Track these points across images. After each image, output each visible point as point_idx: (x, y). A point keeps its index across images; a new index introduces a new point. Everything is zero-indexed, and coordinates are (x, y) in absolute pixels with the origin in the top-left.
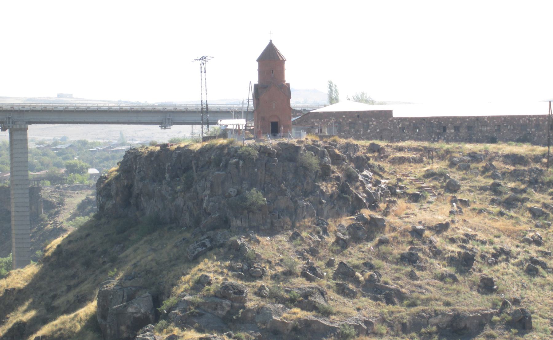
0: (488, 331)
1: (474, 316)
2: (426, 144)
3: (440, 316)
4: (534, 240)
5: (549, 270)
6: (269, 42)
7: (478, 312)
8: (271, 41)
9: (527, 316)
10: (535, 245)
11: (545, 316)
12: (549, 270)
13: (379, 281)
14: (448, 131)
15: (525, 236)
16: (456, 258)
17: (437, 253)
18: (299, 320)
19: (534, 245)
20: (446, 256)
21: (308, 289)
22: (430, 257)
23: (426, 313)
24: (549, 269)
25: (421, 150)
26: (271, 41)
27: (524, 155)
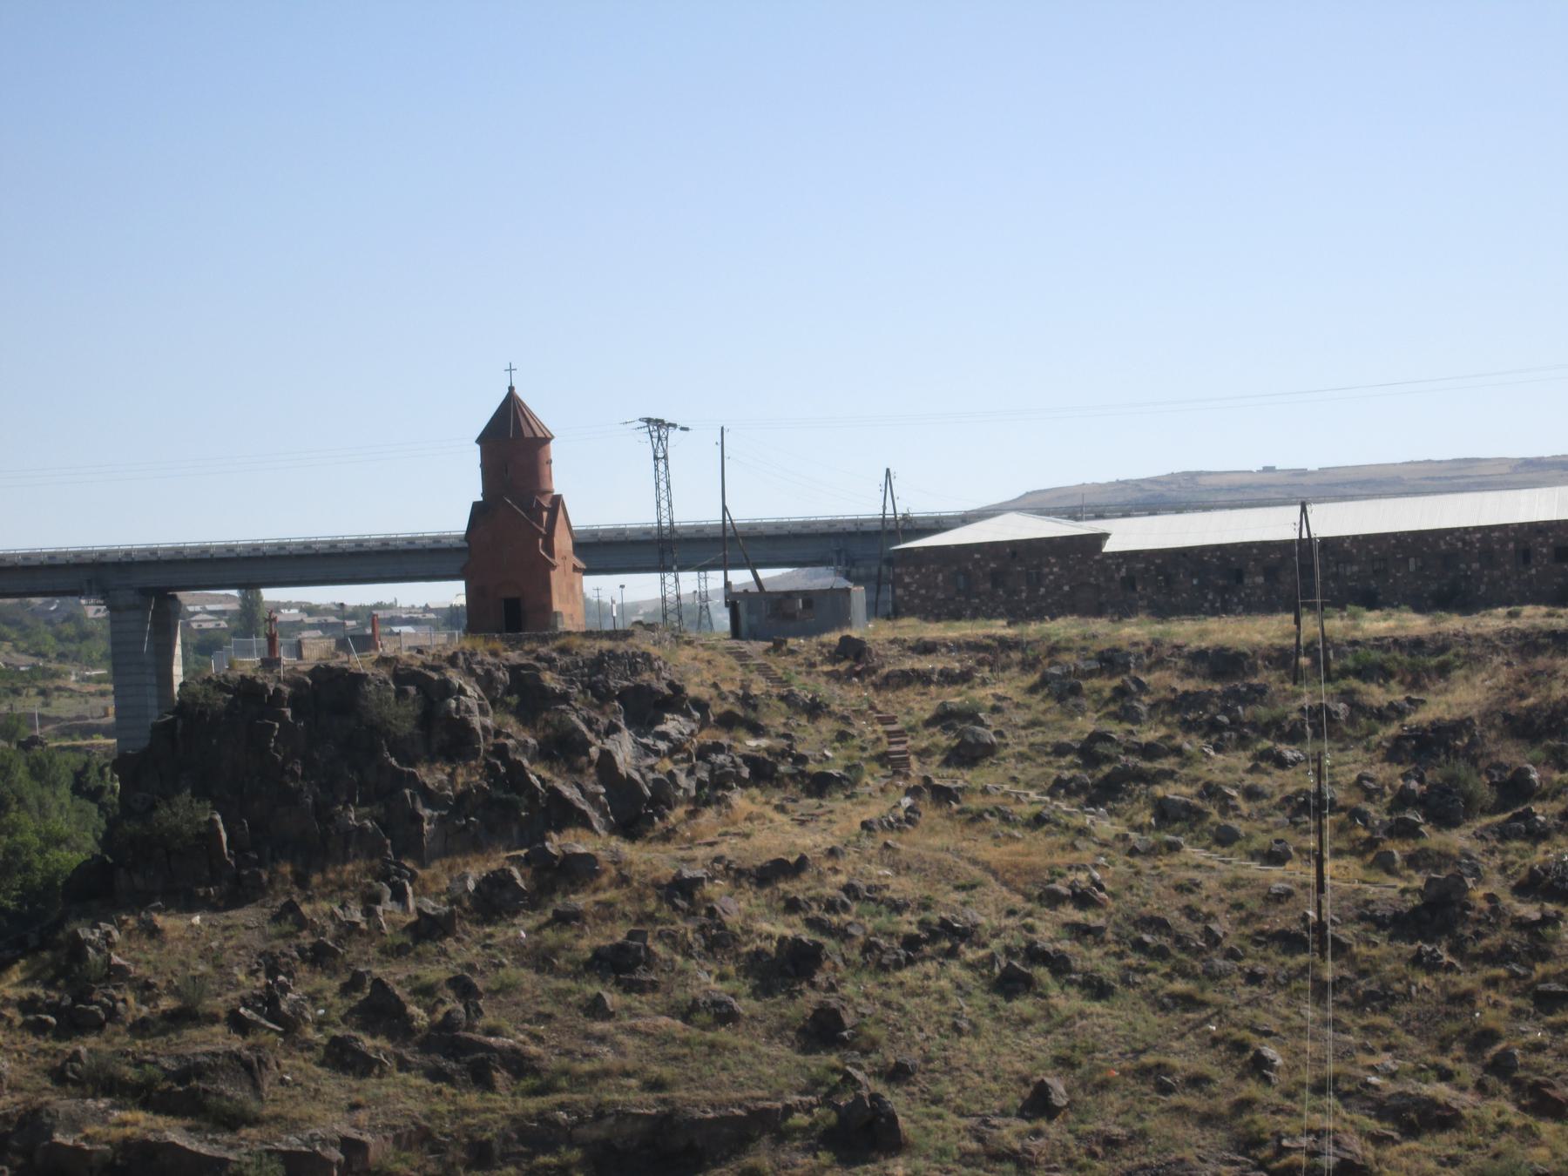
0: (761, 1157)
1: (722, 1117)
2: (999, 628)
3: (611, 1121)
4: (1074, 892)
5: (1074, 976)
6: (502, 395)
7: (740, 1106)
8: (511, 389)
9: (882, 1115)
10: (1075, 907)
11: (969, 1110)
12: (1074, 976)
13: (470, 1028)
14: (1246, 581)
15: (1053, 882)
16: (768, 954)
17: (718, 940)
18: (126, 1145)
19: (1071, 906)
20: (745, 949)
21: (200, 1059)
22: (688, 955)
23: (568, 1113)
24: (1076, 973)
25: (986, 648)
26: (511, 389)
27: (1244, 649)
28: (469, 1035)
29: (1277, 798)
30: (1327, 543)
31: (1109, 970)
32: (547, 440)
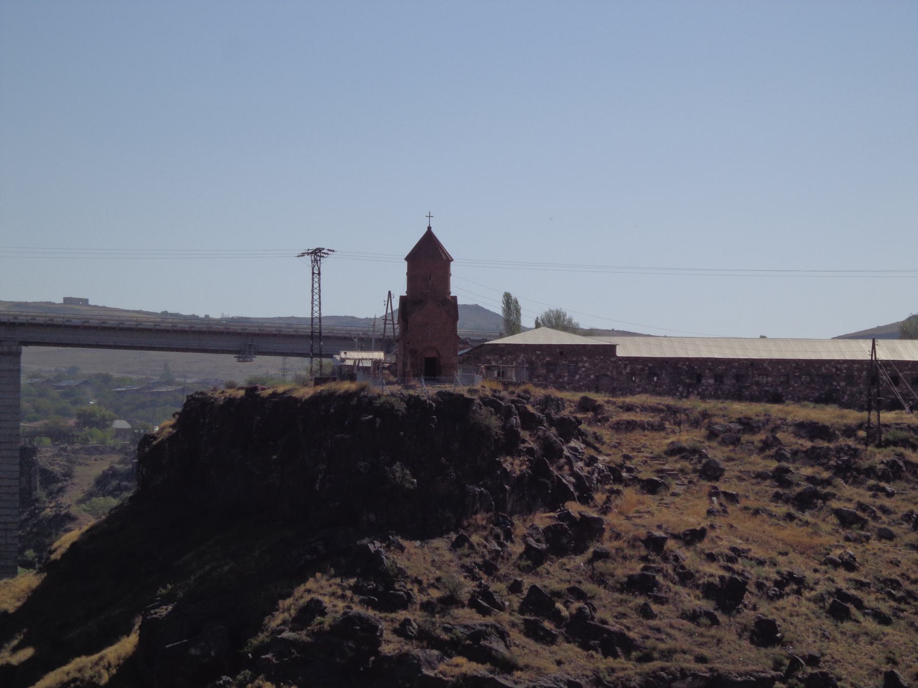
2: (669, 401)
3: (690, 679)
4: (843, 561)
5: (867, 611)
7: (751, 675)
8: (429, 228)
12: (867, 611)
13: (593, 618)
14: (703, 381)
15: (829, 554)
17: (686, 577)
18: (464, 676)
19: (843, 569)
20: (701, 582)
21: (479, 628)
22: (675, 583)
23: (666, 673)
24: (867, 609)
25: (661, 411)
26: (429, 228)
27: (828, 424)
28: (591, 622)
29: (900, 515)
30: (887, 364)
31: (885, 607)
32: (452, 260)
